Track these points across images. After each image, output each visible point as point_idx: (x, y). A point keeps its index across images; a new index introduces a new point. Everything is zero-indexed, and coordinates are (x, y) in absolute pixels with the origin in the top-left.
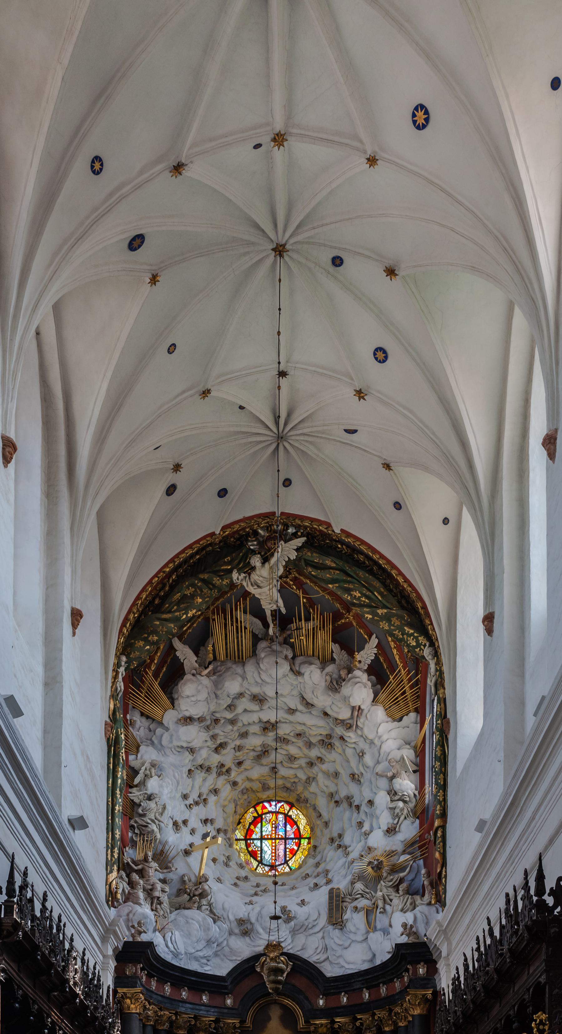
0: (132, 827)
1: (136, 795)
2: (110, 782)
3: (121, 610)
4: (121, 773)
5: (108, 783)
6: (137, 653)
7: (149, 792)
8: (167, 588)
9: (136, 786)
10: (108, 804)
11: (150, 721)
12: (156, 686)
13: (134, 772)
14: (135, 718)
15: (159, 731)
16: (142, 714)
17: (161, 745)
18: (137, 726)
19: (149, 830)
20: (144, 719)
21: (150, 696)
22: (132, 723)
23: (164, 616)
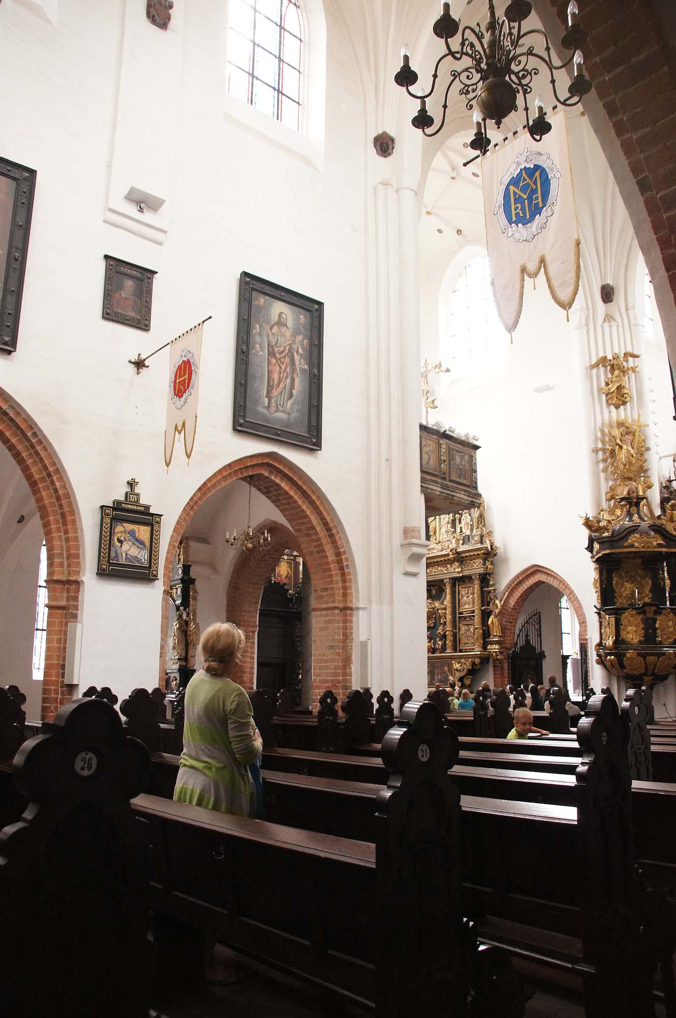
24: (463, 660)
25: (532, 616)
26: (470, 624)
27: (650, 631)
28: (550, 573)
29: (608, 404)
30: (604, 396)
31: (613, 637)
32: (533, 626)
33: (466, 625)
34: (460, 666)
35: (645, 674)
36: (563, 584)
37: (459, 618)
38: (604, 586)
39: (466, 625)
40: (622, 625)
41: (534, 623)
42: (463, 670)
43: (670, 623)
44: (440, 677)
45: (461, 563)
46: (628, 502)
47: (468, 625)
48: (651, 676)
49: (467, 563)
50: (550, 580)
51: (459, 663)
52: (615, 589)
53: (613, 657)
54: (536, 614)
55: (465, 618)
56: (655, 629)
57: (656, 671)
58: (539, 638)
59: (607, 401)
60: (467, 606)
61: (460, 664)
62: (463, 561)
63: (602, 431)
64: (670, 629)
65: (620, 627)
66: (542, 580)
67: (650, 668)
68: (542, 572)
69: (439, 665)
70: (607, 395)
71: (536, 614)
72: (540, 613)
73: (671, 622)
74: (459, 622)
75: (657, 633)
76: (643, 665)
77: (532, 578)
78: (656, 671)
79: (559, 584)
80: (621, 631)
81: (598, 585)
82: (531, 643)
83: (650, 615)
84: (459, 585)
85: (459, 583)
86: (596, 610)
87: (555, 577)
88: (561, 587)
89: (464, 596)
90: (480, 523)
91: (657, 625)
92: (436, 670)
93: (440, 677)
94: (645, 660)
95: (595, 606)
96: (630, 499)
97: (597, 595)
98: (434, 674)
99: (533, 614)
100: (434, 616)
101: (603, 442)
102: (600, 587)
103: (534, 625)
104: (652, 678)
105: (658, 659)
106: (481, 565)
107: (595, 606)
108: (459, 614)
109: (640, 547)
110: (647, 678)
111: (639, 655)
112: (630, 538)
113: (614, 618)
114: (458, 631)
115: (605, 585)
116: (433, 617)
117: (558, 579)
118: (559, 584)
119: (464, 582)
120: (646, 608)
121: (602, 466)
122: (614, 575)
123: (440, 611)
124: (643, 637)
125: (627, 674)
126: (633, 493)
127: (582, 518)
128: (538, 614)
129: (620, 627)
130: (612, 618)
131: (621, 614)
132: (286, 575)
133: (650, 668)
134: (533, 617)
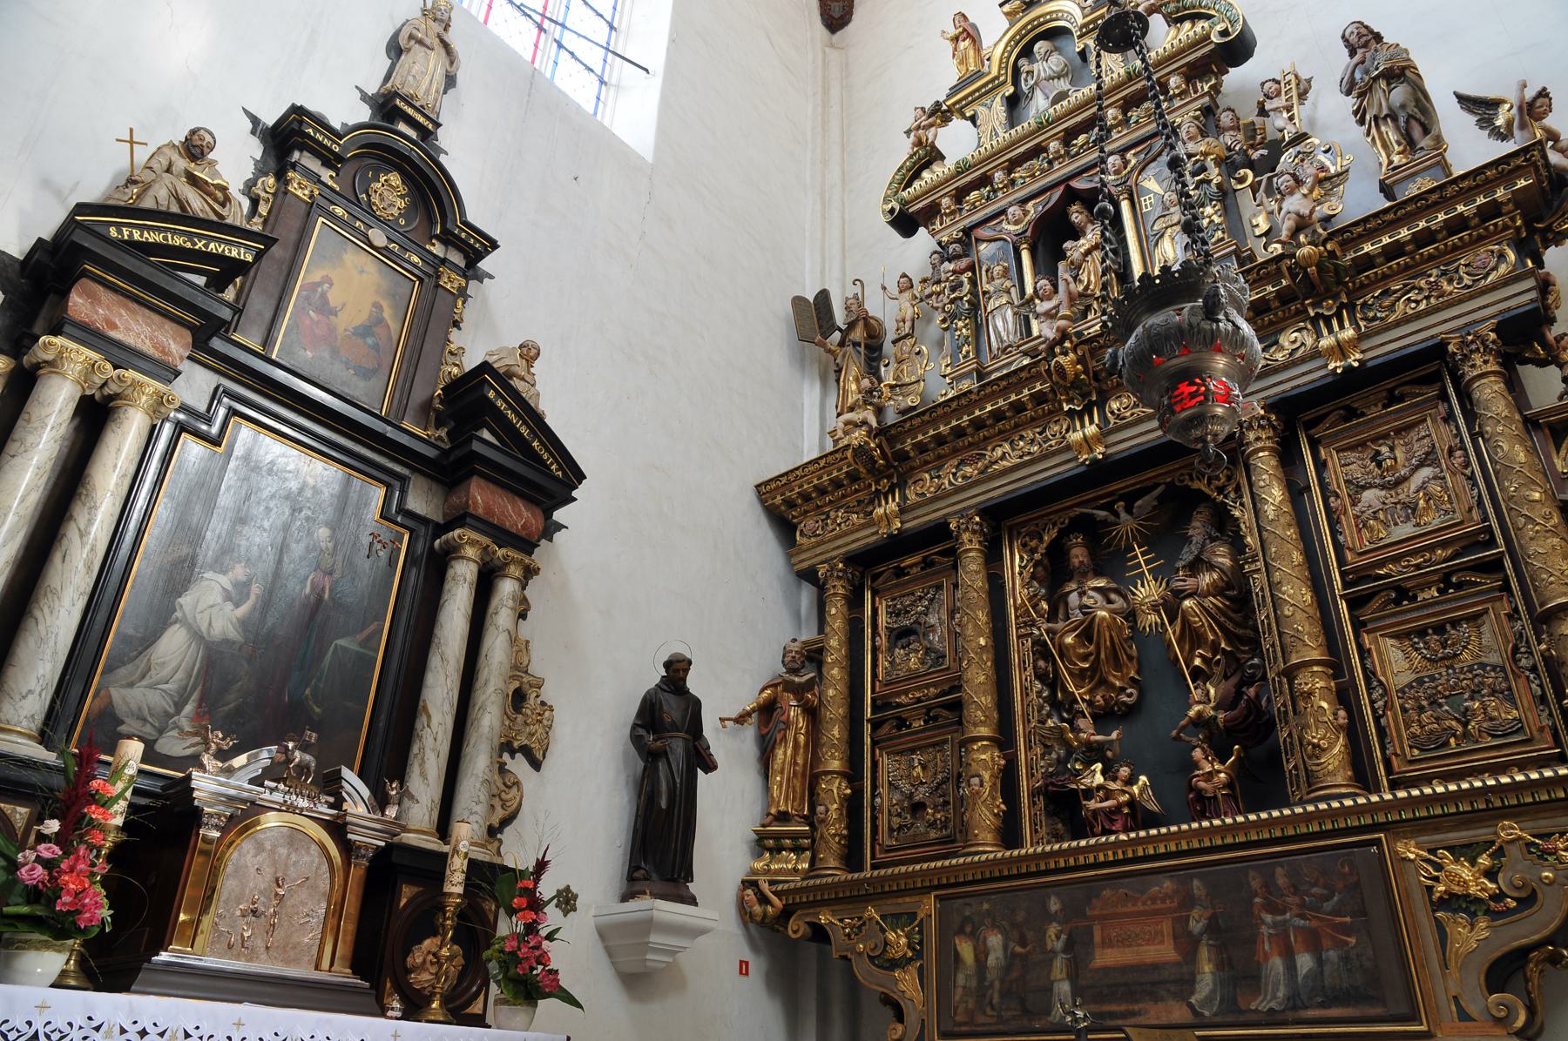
24: (1509, 830)
26: (1455, 623)
33: (1422, 633)
34: (1491, 874)
37: (1355, 603)
39: (1422, 633)
42: (1528, 900)
44: (1305, 962)
45: (1351, 307)
47: (1439, 629)
49: (1386, 293)
51: (1465, 852)
55: (1402, 593)
60: (1405, 530)
61: (1484, 860)
62: (1364, 288)
69: (1281, 880)
74: (1358, 626)
84: (1314, 445)
85: (1318, 433)
89: (1364, 488)
90: (1417, 131)
92: (1268, 918)
93: (1305, 962)
98: (1252, 940)
100: (1134, 651)
106: (1503, 269)
108: (1346, 585)
114: (1359, 673)
116: (1130, 658)
119: (1351, 413)
123: (1187, 603)
132: (362, 317)
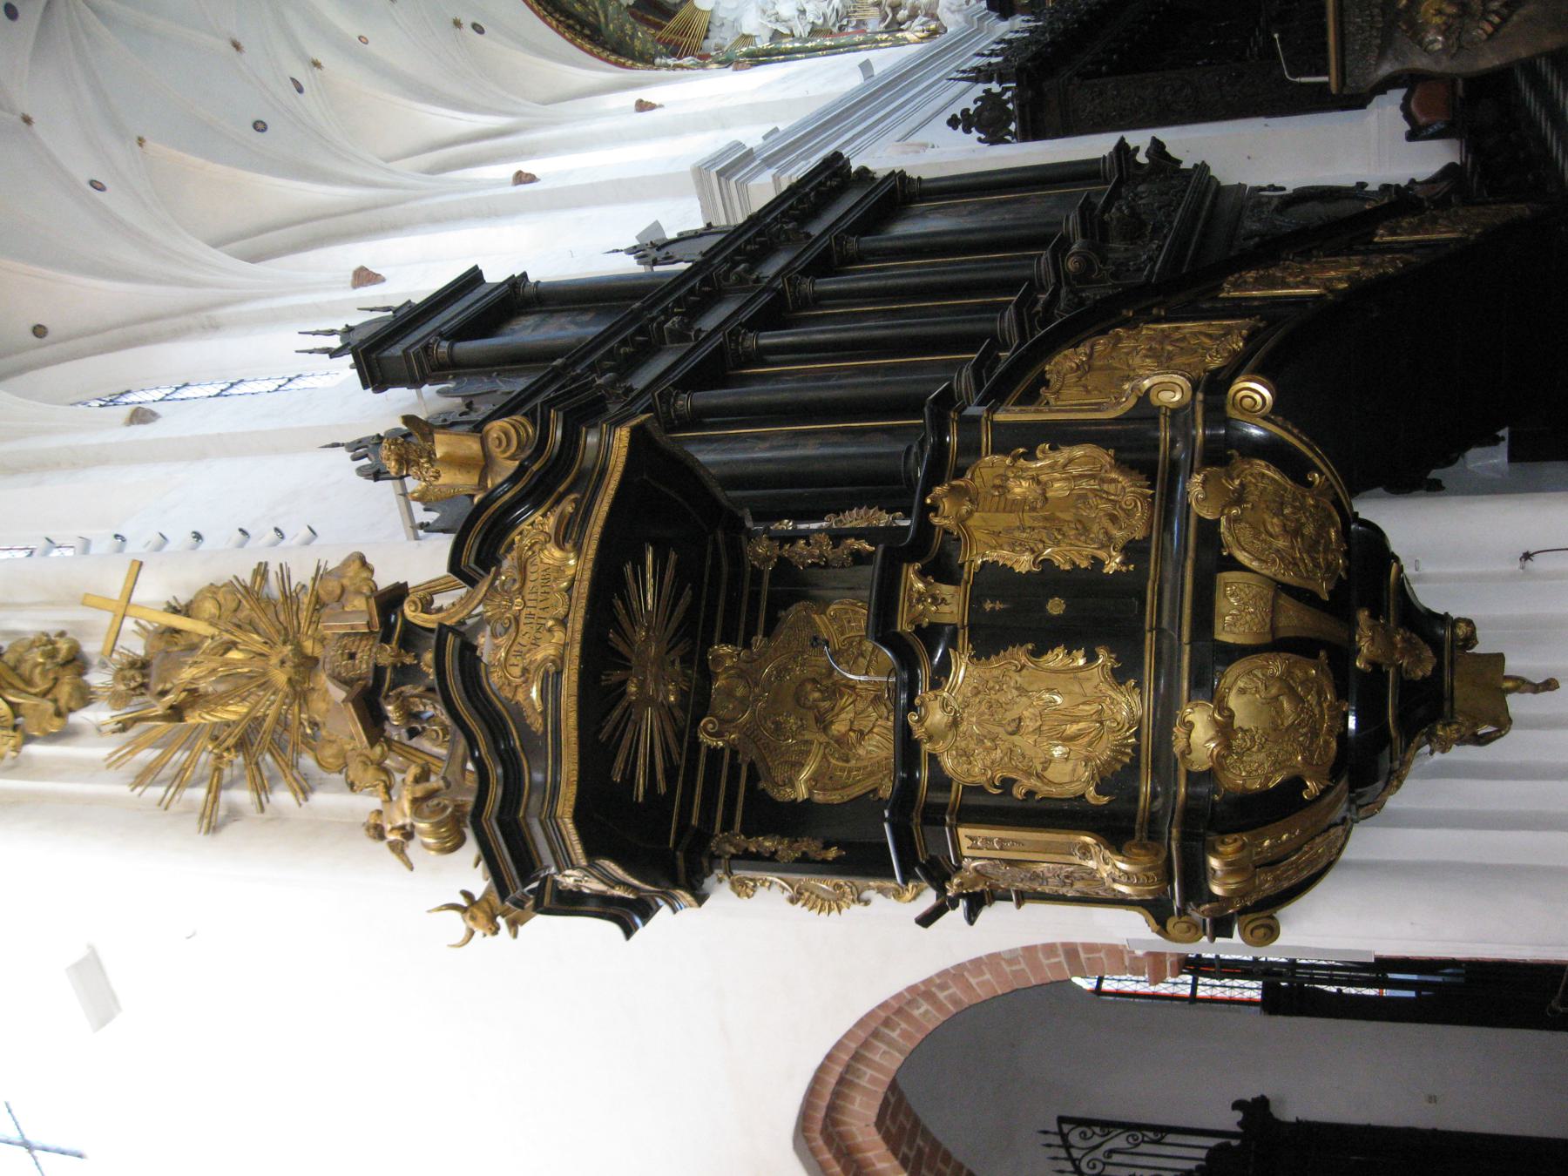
0: (840, 28)
1: (801, 29)
2: (799, 56)
3: (609, 71)
4: (787, 44)
5: (802, 58)
6: (649, 45)
7: (796, 14)
8: (571, 22)
9: (792, 31)
10: (827, 55)
11: (711, 27)
12: (672, 24)
13: (776, 35)
14: (713, 46)
15: (721, 13)
16: (706, 37)
17: (736, 8)
18: (720, 41)
19: (841, 6)
20: (711, 34)
21: (684, 30)
22: (719, 48)
23: (602, 19)
25: (1070, 1158)
27: (1056, 607)
28: (832, 1080)
29: (66, 734)
30: (33, 749)
31: (1085, 851)
32: (1116, 1158)
35: (1340, 657)
36: (887, 1023)
38: (833, 853)
40: (1007, 784)
41: (1099, 1154)
43: (1020, 488)
46: (394, 686)
48: (1352, 624)
50: (873, 1080)
52: (857, 791)
53: (1214, 863)
54: (1064, 1136)
56: (1048, 578)
57: (1324, 590)
58: (1170, 1138)
59: (51, 738)
63: (145, 777)
64: (1059, 489)
65: (1019, 792)
66: (872, 1114)
67: (1294, 619)
68: (832, 1108)
70: (29, 739)
71: (1064, 1136)
72: (1062, 1120)
73: (1011, 483)
75: (1075, 566)
76: (1276, 666)
77: (870, 1154)
78: (1324, 590)
79: (890, 1043)
80: (1044, 790)
81: (824, 884)
82: (1191, 1165)
83: (951, 605)
86: (957, 915)
87: (856, 1057)
88: (905, 1035)
91: (1023, 563)
94: (1232, 654)
95: (926, 920)
96: (379, 671)
97: (877, 899)
99: (1062, 1153)
101: (180, 780)
102: (840, 873)
103: (1111, 1152)
104: (1363, 616)
105: (1233, 565)
107: (926, 920)
109: (559, 636)
110: (1364, 646)
111: (1204, 686)
112: (507, 693)
113: (963, 832)
115: (827, 846)
117: (865, 1044)
118: (890, 1043)
120: (904, 626)
121: (283, 797)
122: (787, 794)
124: (1091, 657)
125: (1335, 772)
126: (352, 656)
127: (472, 933)
128: (1066, 1128)
129: (1019, 792)
130: (965, 843)
131: (941, 781)
133: (1294, 619)
134: (1076, 1154)
